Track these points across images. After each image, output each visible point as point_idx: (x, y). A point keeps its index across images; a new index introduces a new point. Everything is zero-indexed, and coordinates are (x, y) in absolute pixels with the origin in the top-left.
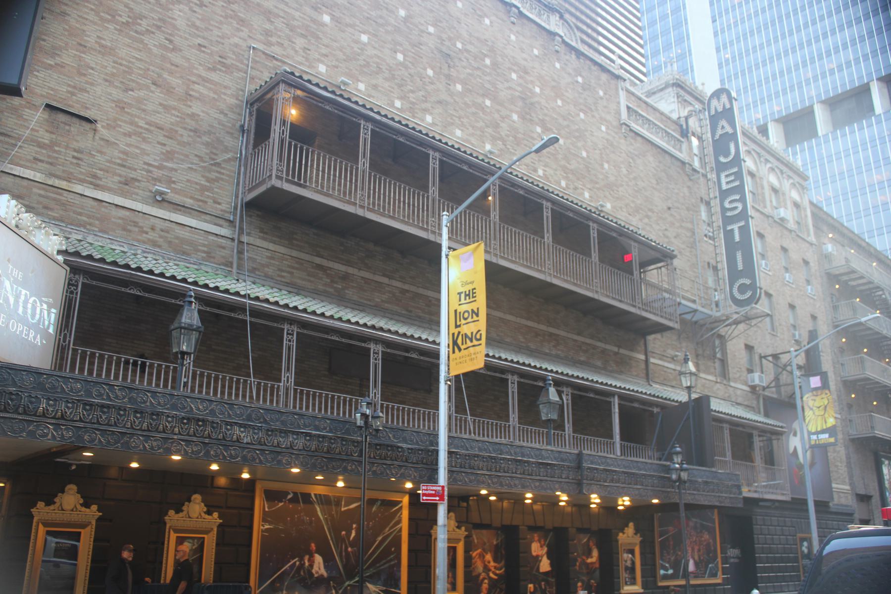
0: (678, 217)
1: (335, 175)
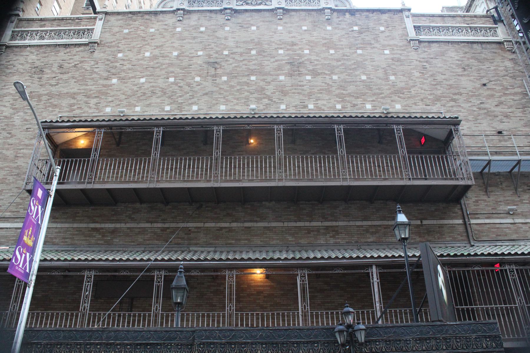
0: (498, 88)
1: (140, 168)
